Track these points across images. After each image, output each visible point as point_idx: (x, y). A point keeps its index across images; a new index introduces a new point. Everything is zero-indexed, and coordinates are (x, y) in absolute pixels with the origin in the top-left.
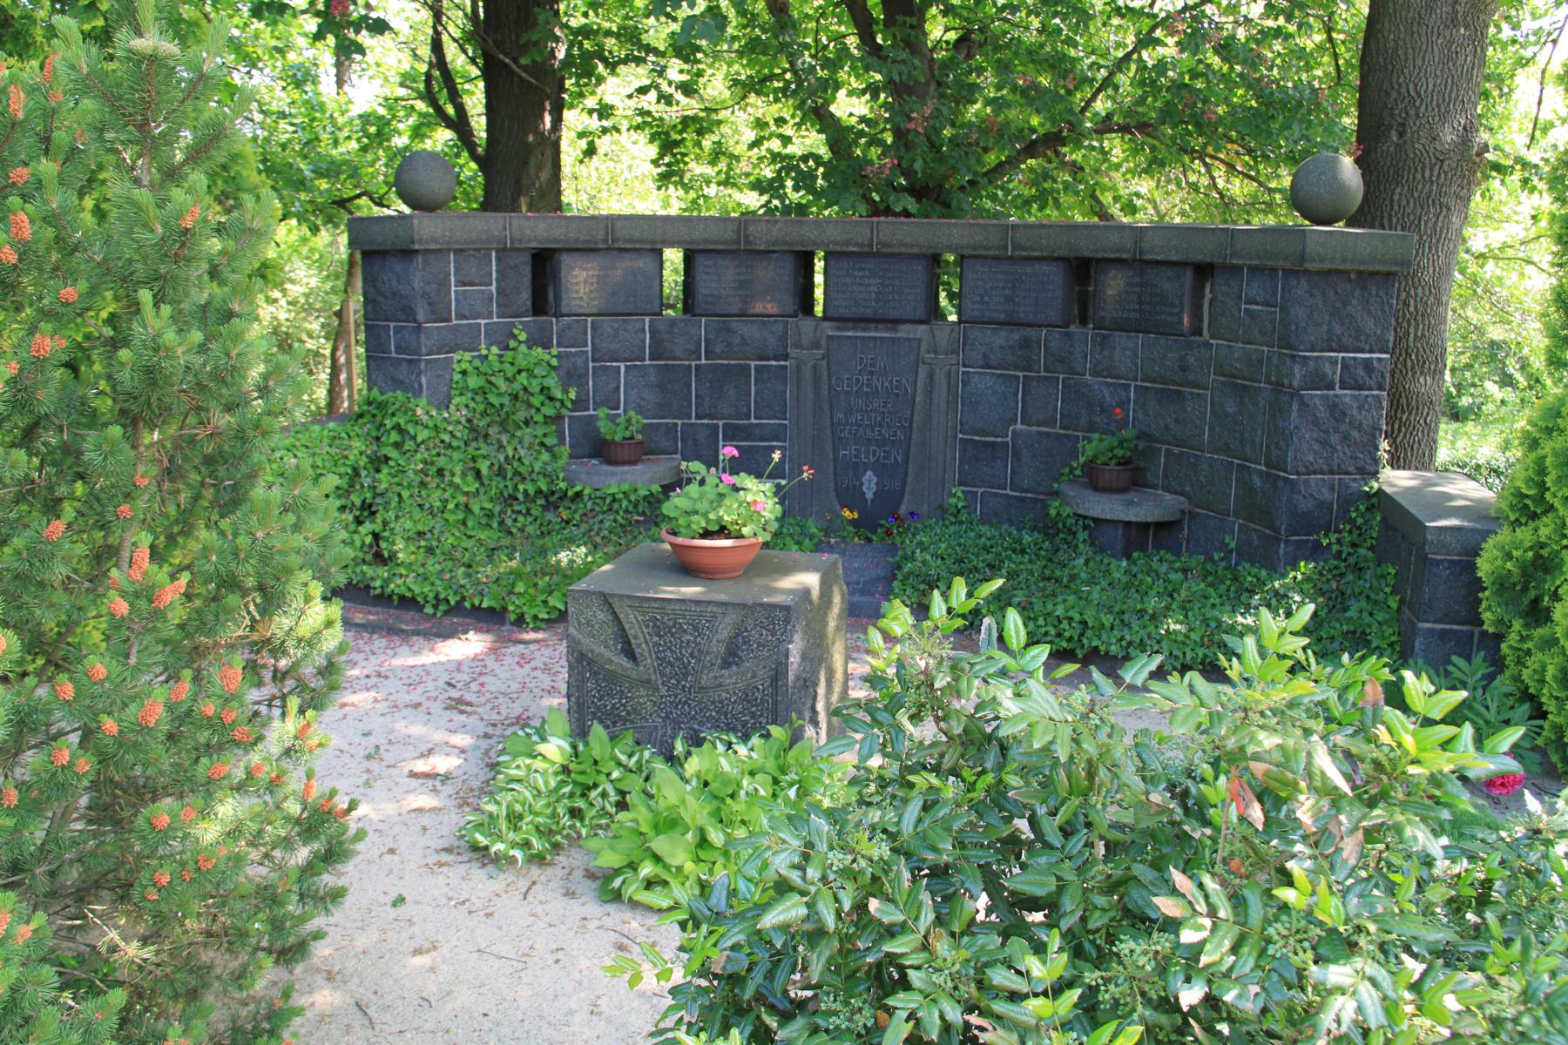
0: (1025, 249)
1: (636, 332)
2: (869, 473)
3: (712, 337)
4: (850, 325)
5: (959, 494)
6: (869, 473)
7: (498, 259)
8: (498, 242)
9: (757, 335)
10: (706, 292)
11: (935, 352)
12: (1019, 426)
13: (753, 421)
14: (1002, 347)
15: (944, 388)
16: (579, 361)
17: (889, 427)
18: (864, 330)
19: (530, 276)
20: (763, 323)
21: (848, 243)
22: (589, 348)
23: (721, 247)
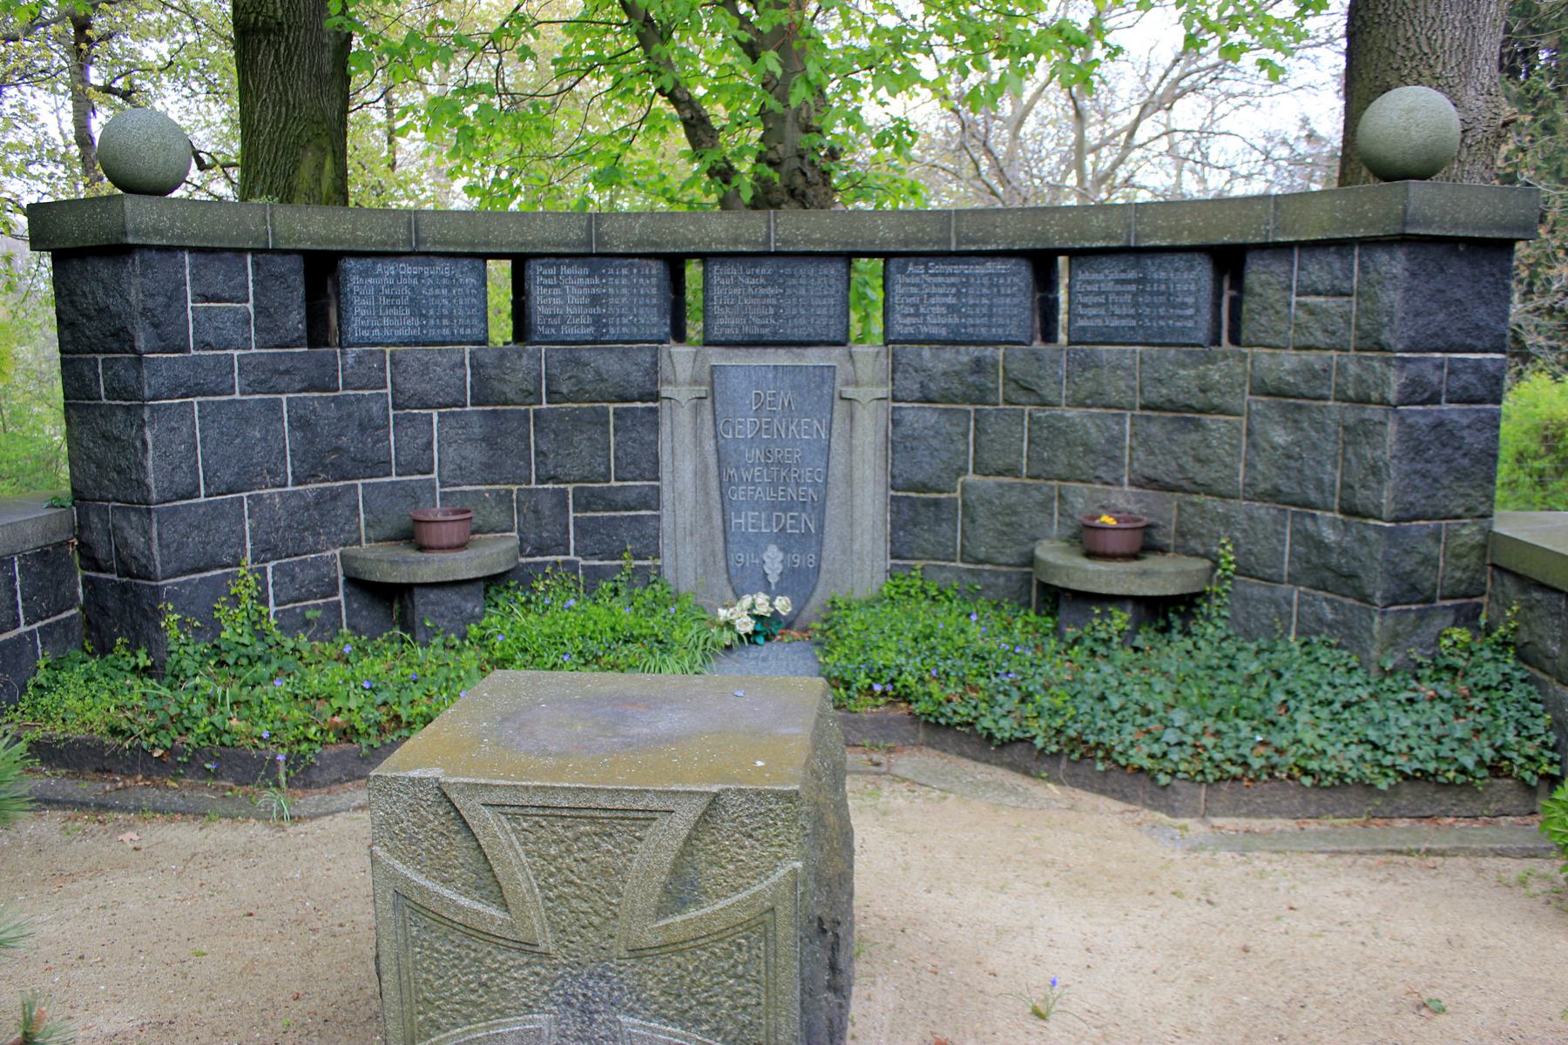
0: (974, 242)
1: (453, 368)
3: (554, 371)
7: (256, 264)
8: (256, 240)
9: (617, 367)
10: (548, 311)
12: (971, 477)
13: (614, 483)
16: (375, 408)
19: (302, 290)
20: (624, 352)
21: (736, 241)
22: (389, 390)
23: (563, 250)
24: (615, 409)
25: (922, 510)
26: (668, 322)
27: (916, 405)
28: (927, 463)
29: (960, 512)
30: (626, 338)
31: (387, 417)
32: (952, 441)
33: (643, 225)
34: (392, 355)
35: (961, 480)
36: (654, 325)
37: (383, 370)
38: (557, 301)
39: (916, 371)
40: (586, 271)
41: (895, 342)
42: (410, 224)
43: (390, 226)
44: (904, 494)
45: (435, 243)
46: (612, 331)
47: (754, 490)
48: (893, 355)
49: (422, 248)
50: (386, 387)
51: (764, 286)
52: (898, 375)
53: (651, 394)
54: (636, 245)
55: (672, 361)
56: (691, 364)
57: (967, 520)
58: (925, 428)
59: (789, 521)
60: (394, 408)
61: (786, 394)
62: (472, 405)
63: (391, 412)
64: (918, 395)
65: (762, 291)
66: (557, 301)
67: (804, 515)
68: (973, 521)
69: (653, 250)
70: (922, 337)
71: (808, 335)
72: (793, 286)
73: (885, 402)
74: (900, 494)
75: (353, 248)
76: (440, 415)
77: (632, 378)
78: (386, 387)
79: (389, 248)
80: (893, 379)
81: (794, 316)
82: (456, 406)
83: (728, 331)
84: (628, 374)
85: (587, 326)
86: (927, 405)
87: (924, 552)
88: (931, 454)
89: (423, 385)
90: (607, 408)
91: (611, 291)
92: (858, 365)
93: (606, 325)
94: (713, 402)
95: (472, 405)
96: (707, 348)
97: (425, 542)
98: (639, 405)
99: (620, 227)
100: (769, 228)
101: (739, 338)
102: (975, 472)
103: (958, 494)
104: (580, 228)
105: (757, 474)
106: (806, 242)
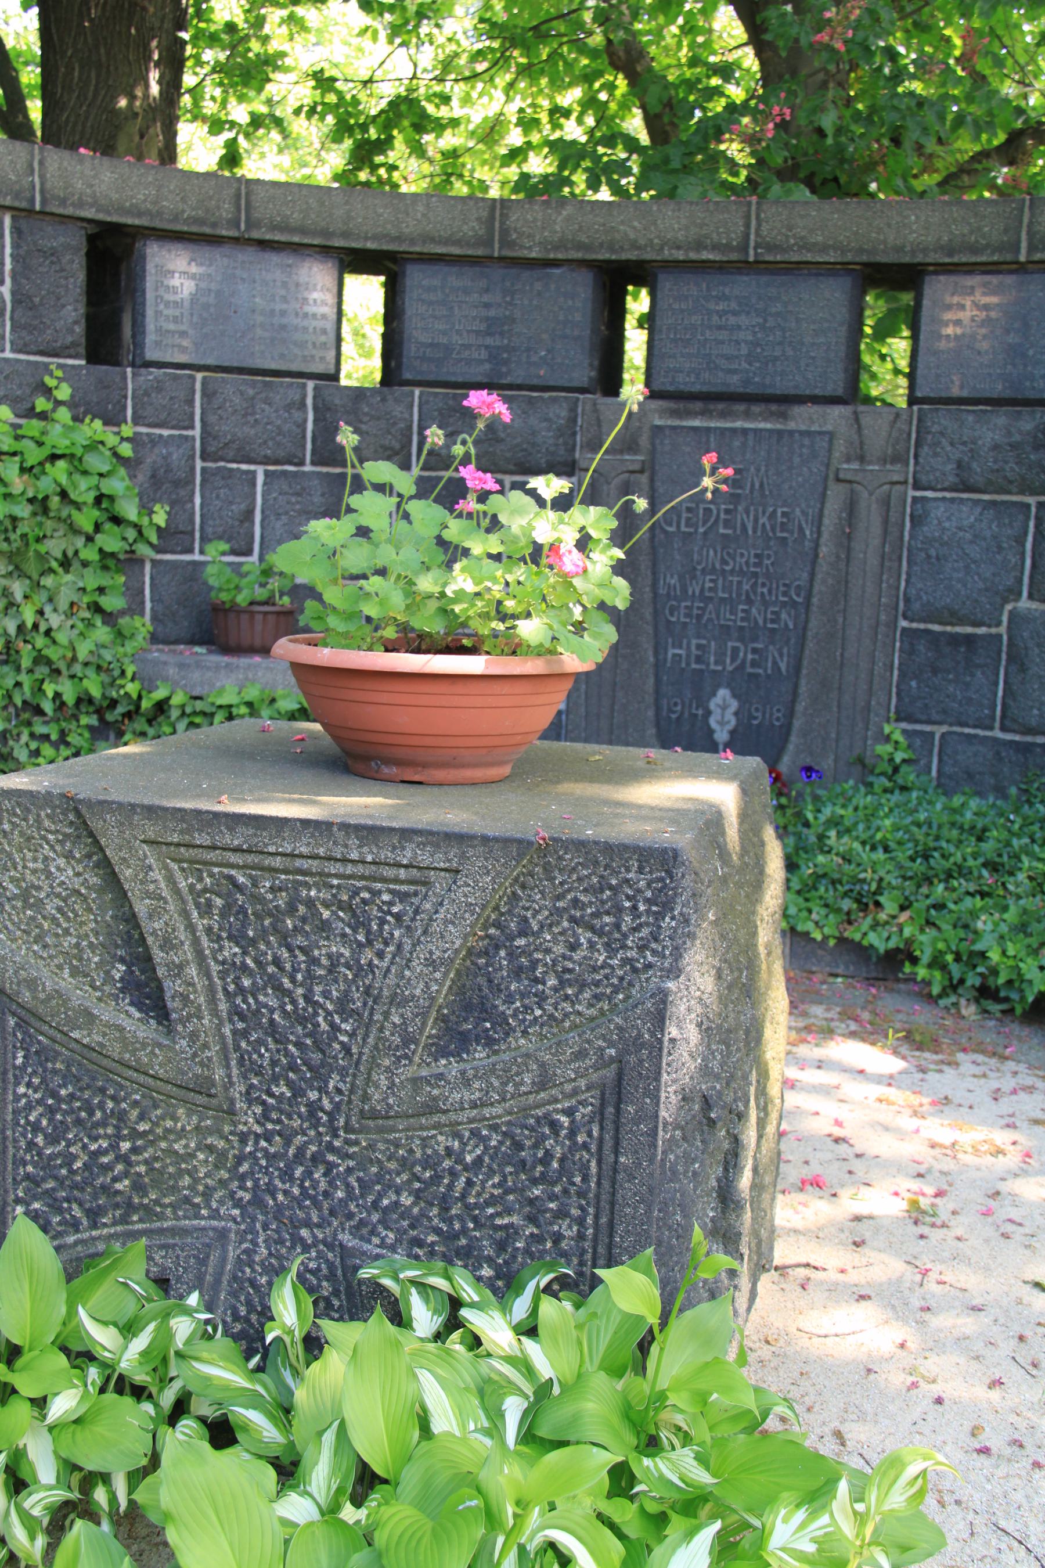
1: (288, 407)
2: (723, 693)
4: (698, 405)
5: (897, 736)
6: (723, 693)
7: (16, 231)
8: (17, 196)
10: (424, 338)
11: (862, 459)
12: (1024, 603)
14: (996, 447)
15: (876, 529)
16: (176, 455)
17: (766, 604)
18: (723, 415)
19: (81, 276)
20: (530, 401)
21: (699, 246)
22: (197, 432)
23: (456, 250)
27: (948, 495)
28: (959, 581)
29: (1004, 656)
31: (193, 469)
32: (1000, 548)
33: (568, 219)
34: (205, 382)
35: (1009, 607)
37: (191, 402)
38: (440, 326)
39: (952, 444)
40: (483, 283)
42: (238, 196)
43: (211, 198)
44: (922, 626)
45: (274, 228)
47: (703, 609)
49: (256, 235)
50: (192, 427)
51: (735, 313)
54: (556, 248)
57: (1013, 668)
58: (960, 529)
59: (750, 656)
60: (203, 459)
61: (758, 470)
62: (313, 463)
63: (199, 464)
64: (952, 479)
65: (732, 320)
66: (440, 326)
68: (1023, 669)
69: (579, 255)
72: (778, 314)
74: (915, 625)
75: (157, 224)
76: (267, 473)
78: (192, 427)
79: (207, 230)
81: (776, 359)
82: (291, 463)
83: (680, 378)
84: (533, 433)
85: (481, 362)
86: (965, 496)
87: (944, 712)
88: (967, 567)
89: (246, 429)
91: (518, 314)
93: (506, 362)
95: (313, 463)
97: (232, 643)
99: (535, 220)
100: (748, 226)
101: (697, 388)
102: (1031, 597)
103: (1003, 630)
104: (478, 219)
105: (708, 585)
106: (801, 248)
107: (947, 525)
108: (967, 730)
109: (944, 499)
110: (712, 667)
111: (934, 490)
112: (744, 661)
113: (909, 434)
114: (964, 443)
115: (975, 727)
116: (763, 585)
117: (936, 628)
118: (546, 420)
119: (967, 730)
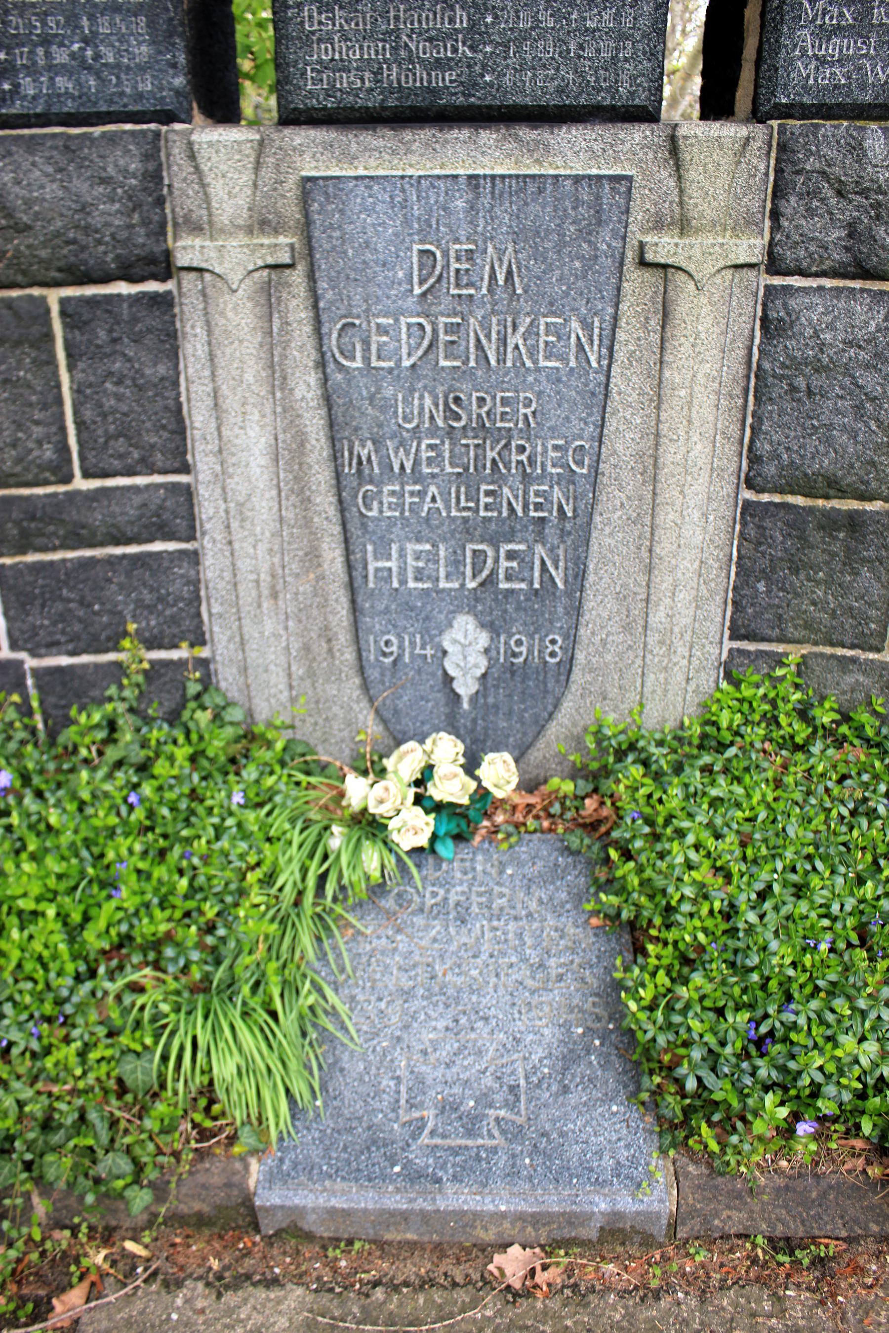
9: (52, 190)
13: (80, 484)
20: (69, 147)
24: (64, 302)
25: (816, 537)
26: (182, 58)
27: (828, 283)
28: (844, 428)
30: (70, 106)
36: (142, 69)
39: (840, 194)
41: (785, 112)
44: (777, 498)
46: (28, 87)
47: (421, 494)
48: (783, 148)
52: (792, 204)
53: (151, 260)
55: (197, 168)
56: (247, 177)
58: (850, 344)
59: (504, 564)
61: (501, 252)
67: (539, 549)
70: (868, 98)
71: (560, 91)
73: (751, 274)
74: (765, 498)
77: (96, 220)
80: (775, 215)
81: (524, 36)
83: (344, 81)
84: (83, 209)
86: (857, 284)
87: (807, 626)
90: (43, 299)
92: (692, 174)
94: (311, 277)
96: (287, 131)
98: (123, 288)
101: (374, 101)
105: (425, 454)
107: (827, 336)
108: (840, 652)
109: (821, 288)
110: (443, 584)
111: (803, 273)
112: (493, 573)
113: (767, 174)
114: (864, 193)
115: (852, 647)
116: (521, 449)
117: (799, 500)
118: (103, 181)
119: (840, 652)
